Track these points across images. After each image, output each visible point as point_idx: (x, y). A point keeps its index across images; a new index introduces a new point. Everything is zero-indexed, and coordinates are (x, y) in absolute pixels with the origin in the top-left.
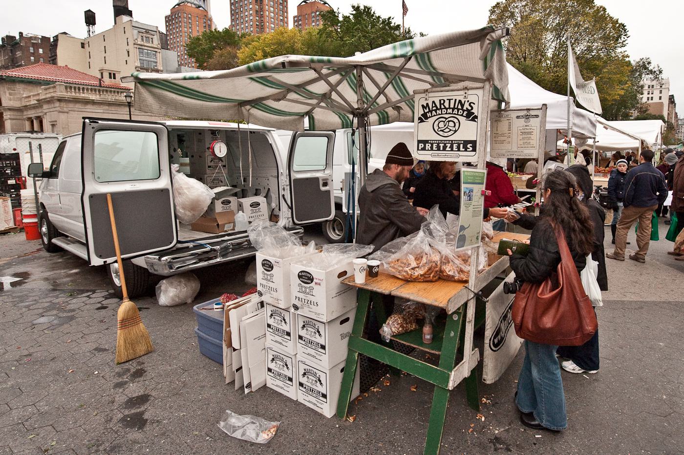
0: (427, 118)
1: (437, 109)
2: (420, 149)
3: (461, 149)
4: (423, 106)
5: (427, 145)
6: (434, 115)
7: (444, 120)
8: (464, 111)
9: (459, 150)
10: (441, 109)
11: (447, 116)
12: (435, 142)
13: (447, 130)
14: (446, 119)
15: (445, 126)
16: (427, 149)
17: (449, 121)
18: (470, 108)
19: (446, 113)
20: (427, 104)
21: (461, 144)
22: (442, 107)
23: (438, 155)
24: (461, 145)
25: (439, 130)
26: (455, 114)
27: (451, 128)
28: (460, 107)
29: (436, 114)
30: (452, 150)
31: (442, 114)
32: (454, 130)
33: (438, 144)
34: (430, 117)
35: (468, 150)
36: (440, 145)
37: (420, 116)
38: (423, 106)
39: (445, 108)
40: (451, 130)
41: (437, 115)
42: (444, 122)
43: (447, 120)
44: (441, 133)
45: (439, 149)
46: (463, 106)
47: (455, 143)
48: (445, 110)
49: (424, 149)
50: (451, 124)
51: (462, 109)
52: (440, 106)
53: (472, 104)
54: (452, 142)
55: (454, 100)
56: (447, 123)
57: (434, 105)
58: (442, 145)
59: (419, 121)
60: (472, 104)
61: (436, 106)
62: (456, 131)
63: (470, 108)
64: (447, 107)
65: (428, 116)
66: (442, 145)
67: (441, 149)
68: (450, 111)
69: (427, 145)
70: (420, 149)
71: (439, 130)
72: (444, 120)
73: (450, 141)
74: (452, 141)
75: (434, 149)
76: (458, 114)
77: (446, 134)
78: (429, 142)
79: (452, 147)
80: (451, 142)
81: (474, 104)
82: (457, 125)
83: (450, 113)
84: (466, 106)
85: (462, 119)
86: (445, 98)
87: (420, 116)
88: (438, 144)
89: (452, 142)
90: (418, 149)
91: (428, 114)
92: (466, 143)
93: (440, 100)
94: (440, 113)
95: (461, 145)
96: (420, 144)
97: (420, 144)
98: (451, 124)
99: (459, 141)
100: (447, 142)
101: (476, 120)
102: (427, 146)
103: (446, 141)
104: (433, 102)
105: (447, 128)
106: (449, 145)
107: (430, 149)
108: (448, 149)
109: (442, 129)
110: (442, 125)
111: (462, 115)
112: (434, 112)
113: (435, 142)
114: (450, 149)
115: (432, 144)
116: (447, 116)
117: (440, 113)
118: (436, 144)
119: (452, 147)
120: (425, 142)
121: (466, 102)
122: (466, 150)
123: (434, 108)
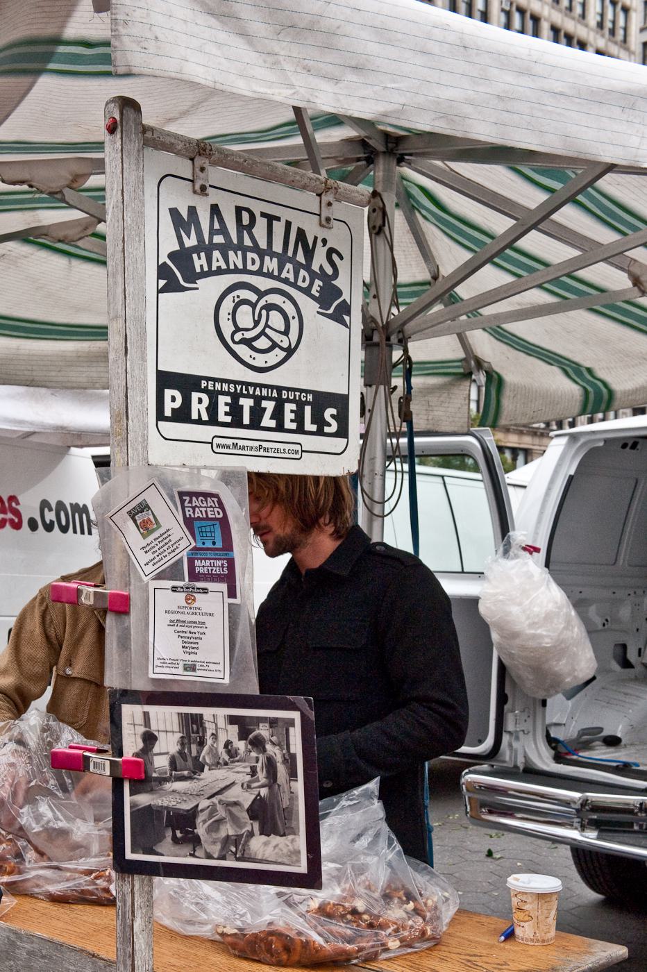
0: (192, 276)
1: (270, 252)
2: (168, 413)
3: (309, 426)
4: (174, 213)
5: (195, 396)
6: (220, 271)
7: (253, 297)
8: (314, 276)
9: (300, 430)
10: (240, 247)
11: (263, 283)
12: (225, 387)
13: (262, 343)
14: (261, 294)
15: (257, 323)
16: (195, 416)
17: (270, 307)
18: (329, 271)
19: (259, 273)
20: (192, 210)
21: (307, 403)
22: (247, 242)
23: (235, 446)
24: (308, 410)
25: (238, 337)
26: (286, 281)
27: (277, 338)
28: (301, 257)
29: (224, 266)
30: (280, 428)
31: (245, 271)
32: (285, 345)
33: (236, 397)
34: (204, 275)
35: (327, 430)
36: (242, 401)
37: (164, 258)
38: (174, 213)
39: (255, 248)
40: (275, 345)
41: (228, 271)
42: (254, 306)
43: (262, 303)
44: (242, 350)
45: (237, 423)
46: (309, 254)
47: (288, 400)
48: (256, 256)
49: (182, 415)
50: (276, 320)
51: (308, 267)
52: (240, 238)
53: (335, 257)
54: (280, 394)
55: (283, 223)
56: (264, 312)
57: (217, 226)
58: (247, 403)
59: (162, 283)
60: (335, 257)
61: (224, 231)
62: (290, 351)
63: (329, 271)
64: (263, 244)
65: (198, 270)
66: (247, 403)
67: (246, 421)
68: (271, 264)
69: (195, 396)
70: (168, 413)
71: (238, 337)
72: (253, 297)
73: (272, 387)
74: (280, 389)
75: (222, 418)
76: (294, 285)
77: (260, 360)
78: (204, 384)
79: (278, 414)
80: (275, 394)
81: (341, 258)
82: (294, 325)
83: (270, 275)
84: (319, 260)
85: (309, 307)
86: (257, 208)
87: (164, 258)
88: (236, 397)
89: (280, 394)
90: (160, 416)
91: (195, 256)
92: (322, 400)
93: (239, 210)
94: (240, 266)
95: (308, 410)
96: (168, 393)
97: (168, 393)
98: (276, 320)
99: (301, 391)
100: (264, 392)
101: (347, 318)
102: (195, 406)
103: (262, 386)
104: (215, 210)
105: (263, 333)
106: (269, 406)
107: (205, 417)
108: (267, 421)
109: (249, 335)
110: (245, 317)
111: (306, 291)
112: (216, 254)
113: (225, 387)
114: (228, 419)
115: (214, 396)
116: (263, 283)
117: (240, 266)
118: (228, 399)
119: (278, 414)
120: (187, 384)
121: (319, 243)
122: (320, 432)
123: (219, 239)
